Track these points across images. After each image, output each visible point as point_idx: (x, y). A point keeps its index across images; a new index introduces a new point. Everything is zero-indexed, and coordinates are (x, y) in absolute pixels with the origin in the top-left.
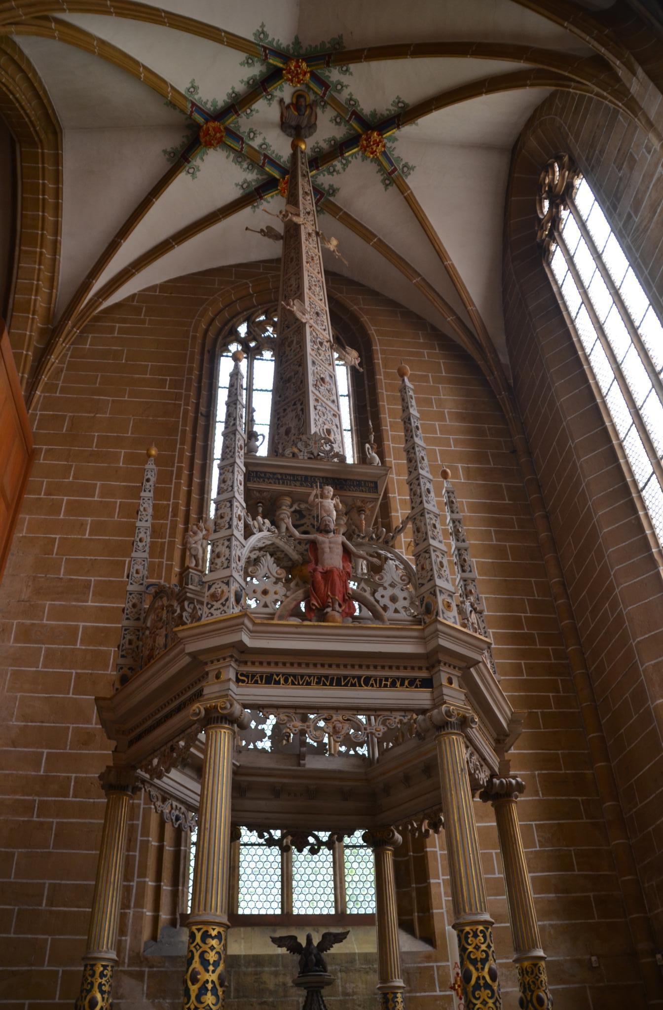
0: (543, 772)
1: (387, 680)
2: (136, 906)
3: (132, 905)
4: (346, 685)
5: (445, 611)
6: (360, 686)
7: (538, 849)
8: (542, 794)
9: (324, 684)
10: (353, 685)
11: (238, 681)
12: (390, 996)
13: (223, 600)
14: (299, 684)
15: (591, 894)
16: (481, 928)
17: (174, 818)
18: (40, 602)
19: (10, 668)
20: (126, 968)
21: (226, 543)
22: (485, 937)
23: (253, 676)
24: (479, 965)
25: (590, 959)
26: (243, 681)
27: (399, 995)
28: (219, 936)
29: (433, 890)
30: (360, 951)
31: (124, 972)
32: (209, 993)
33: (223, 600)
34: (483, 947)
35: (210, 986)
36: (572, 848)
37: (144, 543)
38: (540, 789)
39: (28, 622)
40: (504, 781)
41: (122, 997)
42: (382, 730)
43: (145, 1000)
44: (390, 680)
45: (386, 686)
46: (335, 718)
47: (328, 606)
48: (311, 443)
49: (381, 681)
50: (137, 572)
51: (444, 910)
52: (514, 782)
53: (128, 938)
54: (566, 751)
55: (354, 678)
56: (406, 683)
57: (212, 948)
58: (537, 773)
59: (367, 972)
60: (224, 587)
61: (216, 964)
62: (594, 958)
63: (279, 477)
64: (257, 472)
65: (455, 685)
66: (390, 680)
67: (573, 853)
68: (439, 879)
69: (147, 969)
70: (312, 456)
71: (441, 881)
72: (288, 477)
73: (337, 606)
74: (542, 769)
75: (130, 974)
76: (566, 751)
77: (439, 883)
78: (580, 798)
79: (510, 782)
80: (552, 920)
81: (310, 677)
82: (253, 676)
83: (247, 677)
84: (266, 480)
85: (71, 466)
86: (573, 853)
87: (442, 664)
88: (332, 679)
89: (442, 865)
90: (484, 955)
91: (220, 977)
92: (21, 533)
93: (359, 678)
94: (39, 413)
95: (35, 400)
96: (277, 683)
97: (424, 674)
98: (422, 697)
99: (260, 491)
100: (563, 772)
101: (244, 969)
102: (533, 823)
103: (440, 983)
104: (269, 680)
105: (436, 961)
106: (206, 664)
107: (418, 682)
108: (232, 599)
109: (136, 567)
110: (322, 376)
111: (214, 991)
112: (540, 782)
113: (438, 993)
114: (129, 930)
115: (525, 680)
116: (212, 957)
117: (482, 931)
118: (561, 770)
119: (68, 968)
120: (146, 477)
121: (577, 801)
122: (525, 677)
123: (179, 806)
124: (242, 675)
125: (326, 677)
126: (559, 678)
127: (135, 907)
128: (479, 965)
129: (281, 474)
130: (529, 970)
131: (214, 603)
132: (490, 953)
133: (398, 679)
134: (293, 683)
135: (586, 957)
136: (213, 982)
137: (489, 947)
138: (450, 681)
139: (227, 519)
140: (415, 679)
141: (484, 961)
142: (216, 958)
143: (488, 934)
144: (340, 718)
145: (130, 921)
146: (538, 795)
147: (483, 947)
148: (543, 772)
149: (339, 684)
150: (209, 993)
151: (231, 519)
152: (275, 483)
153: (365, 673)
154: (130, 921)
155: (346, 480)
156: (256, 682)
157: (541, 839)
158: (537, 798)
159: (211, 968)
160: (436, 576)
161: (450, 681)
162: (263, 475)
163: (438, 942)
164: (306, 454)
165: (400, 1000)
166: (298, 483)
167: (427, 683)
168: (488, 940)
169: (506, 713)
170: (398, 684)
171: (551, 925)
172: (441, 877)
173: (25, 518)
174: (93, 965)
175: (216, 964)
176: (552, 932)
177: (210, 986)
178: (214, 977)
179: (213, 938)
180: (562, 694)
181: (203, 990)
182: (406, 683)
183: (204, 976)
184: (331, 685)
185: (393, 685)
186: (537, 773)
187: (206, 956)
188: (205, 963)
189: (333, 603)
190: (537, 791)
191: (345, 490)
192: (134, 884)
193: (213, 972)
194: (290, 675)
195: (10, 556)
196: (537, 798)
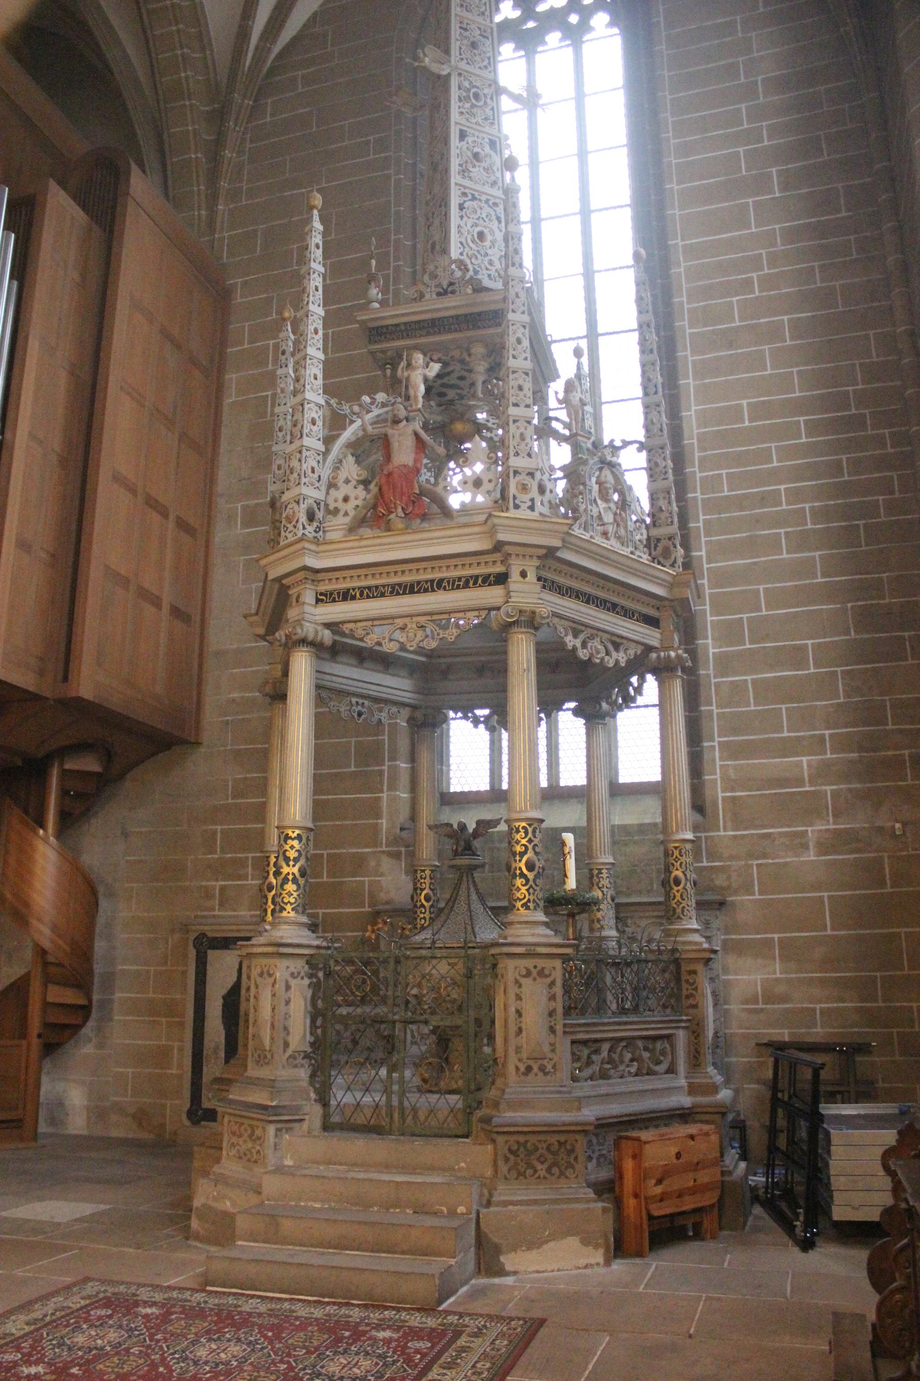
0: (860, 603)
1: (460, 579)
2: (390, 789)
3: (385, 788)
4: (418, 592)
5: (517, 495)
6: (433, 590)
7: (842, 700)
8: (855, 631)
9: (398, 594)
10: (426, 591)
11: (318, 601)
12: (596, 872)
13: (294, 523)
14: (374, 597)
15: (906, 752)
16: (524, 824)
17: (355, 715)
18: (261, 477)
19: (242, 558)
20: (384, 849)
21: (298, 455)
22: (526, 833)
23: (331, 594)
24: (518, 858)
25: (893, 827)
26: (322, 600)
27: (604, 871)
28: (299, 837)
29: (706, 756)
30: (620, 823)
31: (383, 852)
32: (290, 883)
33: (294, 523)
34: (524, 841)
35: (290, 877)
37: (284, 432)
38: (851, 626)
39: (253, 502)
40: (662, 654)
41: (382, 875)
42: (455, 634)
43: (403, 877)
44: (463, 580)
45: (458, 587)
46: (409, 626)
47: (392, 512)
48: (440, 272)
49: (454, 581)
50: (279, 468)
51: (718, 776)
52: (673, 654)
53: (384, 821)
55: (426, 582)
56: (480, 579)
57: (292, 847)
58: (849, 605)
59: (626, 845)
60: (295, 505)
61: (296, 860)
62: (898, 825)
63: (403, 328)
64: (378, 328)
65: (531, 576)
66: (463, 580)
67: (888, 703)
68: (713, 741)
69: (403, 849)
70: (441, 290)
71: (716, 744)
72: (413, 326)
73: (400, 509)
74: (858, 600)
75: (390, 854)
77: (714, 747)
78: (906, 634)
79: (669, 656)
80: (850, 783)
81: (384, 586)
82: (331, 594)
83: (326, 595)
84: (388, 336)
85: (273, 297)
86: (888, 703)
87: (513, 557)
88: (406, 586)
89: (718, 726)
90: (523, 848)
91: (299, 870)
92: (231, 396)
93: (432, 581)
94: (226, 235)
95: (219, 220)
96: (353, 598)
97: (500, 569)
98: (492, 595)
99: (383, 352)
101: (497, 845)
102: (839, 669)
103: (707, 853)
104: (346, 596)
105: (705, 831)
106: (289, 587)
107: (492, 578)
108: (303, 519)
109: (278, 462)
110: (476, 150)
111: (295, 880)
113: (705, 864)
114: (385, 814)
116: (292, 854)
117: (524, 828)
118: (884, 599)
119: (332, 851)
120: (281, 350)
121: (903, 638)
123: (361, 701)
124: (321, 594)
125: (400, 585)
126: (895, 475)
127: (387, 791)
128: (518, 858)
129: (405, 324)
130: (670, 852)
131: (288, 525)
132: (530, 847)
133: (471, 577)
134: (368, 597)
135: (890, 824)
136: (293, 874)
137: (530, 841)
138: (523, 574)
139: (299, 426)
140: (490, 575)
141: (522, 854)
142: (296, 855)
143: (530, 830)
144: (414, 626)
145: (385, 804)
146: (849, 634)
147: (524, 841)
148: (860, 603)
149: (412, 592)
150: (290, 883)
151: (302, 426)
152: (398, 339)
153: (437, 575)
154: (385, 804)
155: (479, 314)
156: (334, 601)
157: (847, 688)
158: (848, 637)
159: (291, 863)
160: (512, 454)
161: (523, 574)
162: (385, 330)
163: (709, 810)
164: (433, 289)
165: (604, 875)
166: (424, 332)
167: (502, 579)
168: (530, 835)
169: (664, 580)
170: (471, 583)
171: (850, 790)
172: (717, 739)
173: (232, 377)
174: (268, 857)
175: (296, 860)
176: (849, 796)
177: (290, 877)
178: (295, 870)
179: (293, 839)
181: (285, 880)
182: (480, 581)
183: (285, 870)
184: (404, 593)
185: (466, 586)
186: (849, 605)
187: (288, 854)
188: (287, 860)
189: (396, 508)
190: (849, 628)
191: (479, 328)
192: (385, 768)
193: (294, 866)
194: (365, 588)
195: (223, 430)
196: (848, 637)
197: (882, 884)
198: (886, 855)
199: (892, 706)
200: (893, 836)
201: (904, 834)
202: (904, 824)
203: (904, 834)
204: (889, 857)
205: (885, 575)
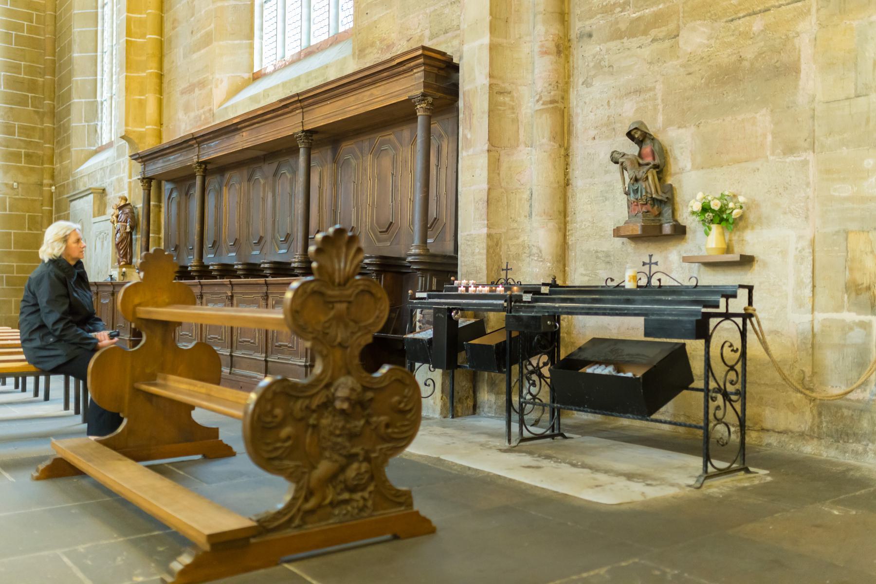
15: (23, 151)
36: (16, 123)
54: (28, 64)
62: (15, 184)
67: (17, 126)
74: (7, 72)
76: (28, 64)
78: (30, 95)
86: (17, 126)
100: (22, 76)
112: (3, 80)
115: (8, 9)
122: (9, 7)
126: (35, 13)
135: (12, 182)
180: (34, 24)
197: (5, 210)
198: (8, 196)
199: (18, 127)
200: (13, 188)
201: (18, 188)
202: (18, 184)
203: (18, 188)
204: (9, 198)
205: (23, 63)
